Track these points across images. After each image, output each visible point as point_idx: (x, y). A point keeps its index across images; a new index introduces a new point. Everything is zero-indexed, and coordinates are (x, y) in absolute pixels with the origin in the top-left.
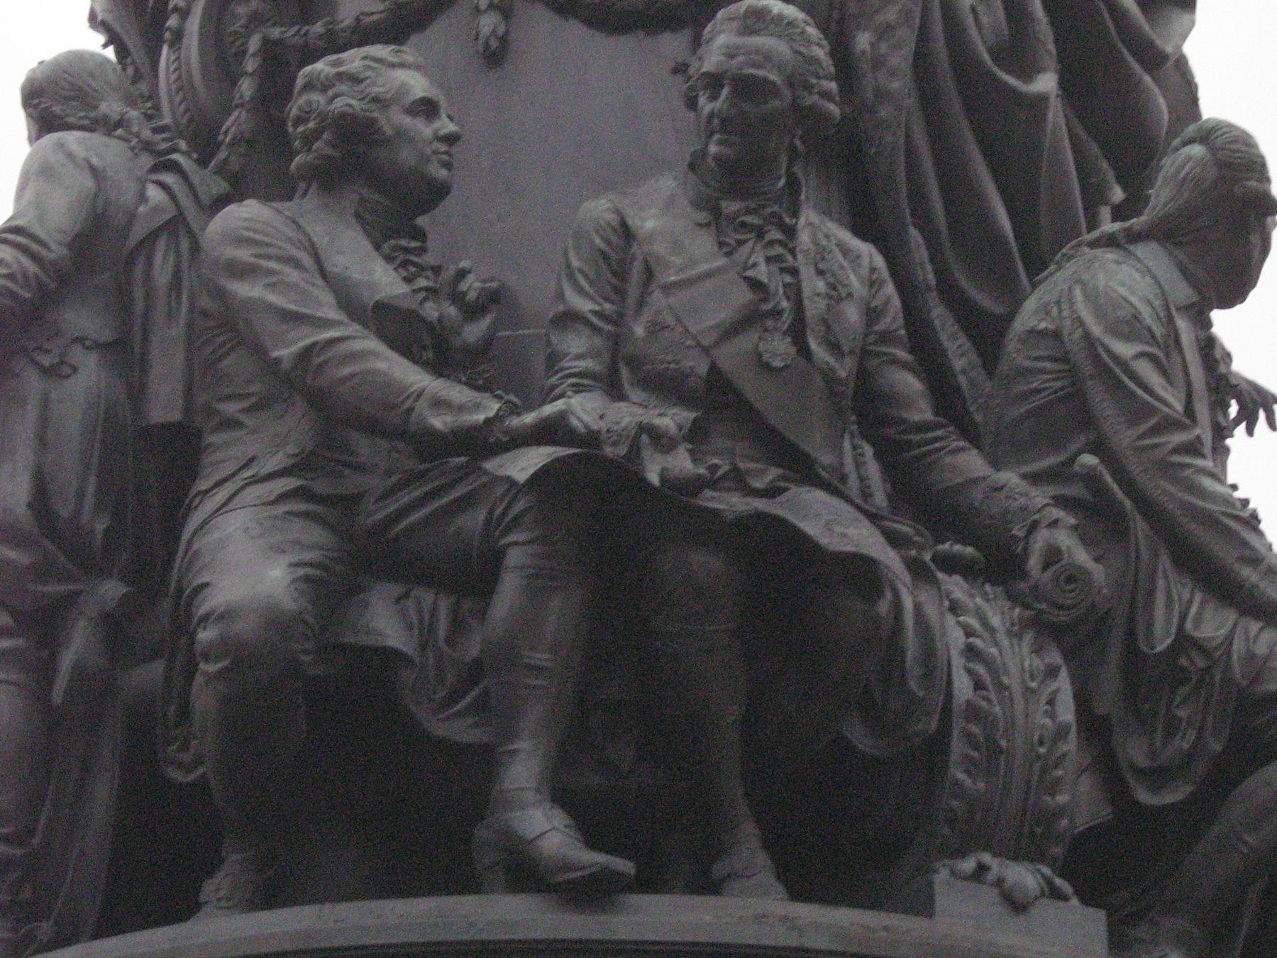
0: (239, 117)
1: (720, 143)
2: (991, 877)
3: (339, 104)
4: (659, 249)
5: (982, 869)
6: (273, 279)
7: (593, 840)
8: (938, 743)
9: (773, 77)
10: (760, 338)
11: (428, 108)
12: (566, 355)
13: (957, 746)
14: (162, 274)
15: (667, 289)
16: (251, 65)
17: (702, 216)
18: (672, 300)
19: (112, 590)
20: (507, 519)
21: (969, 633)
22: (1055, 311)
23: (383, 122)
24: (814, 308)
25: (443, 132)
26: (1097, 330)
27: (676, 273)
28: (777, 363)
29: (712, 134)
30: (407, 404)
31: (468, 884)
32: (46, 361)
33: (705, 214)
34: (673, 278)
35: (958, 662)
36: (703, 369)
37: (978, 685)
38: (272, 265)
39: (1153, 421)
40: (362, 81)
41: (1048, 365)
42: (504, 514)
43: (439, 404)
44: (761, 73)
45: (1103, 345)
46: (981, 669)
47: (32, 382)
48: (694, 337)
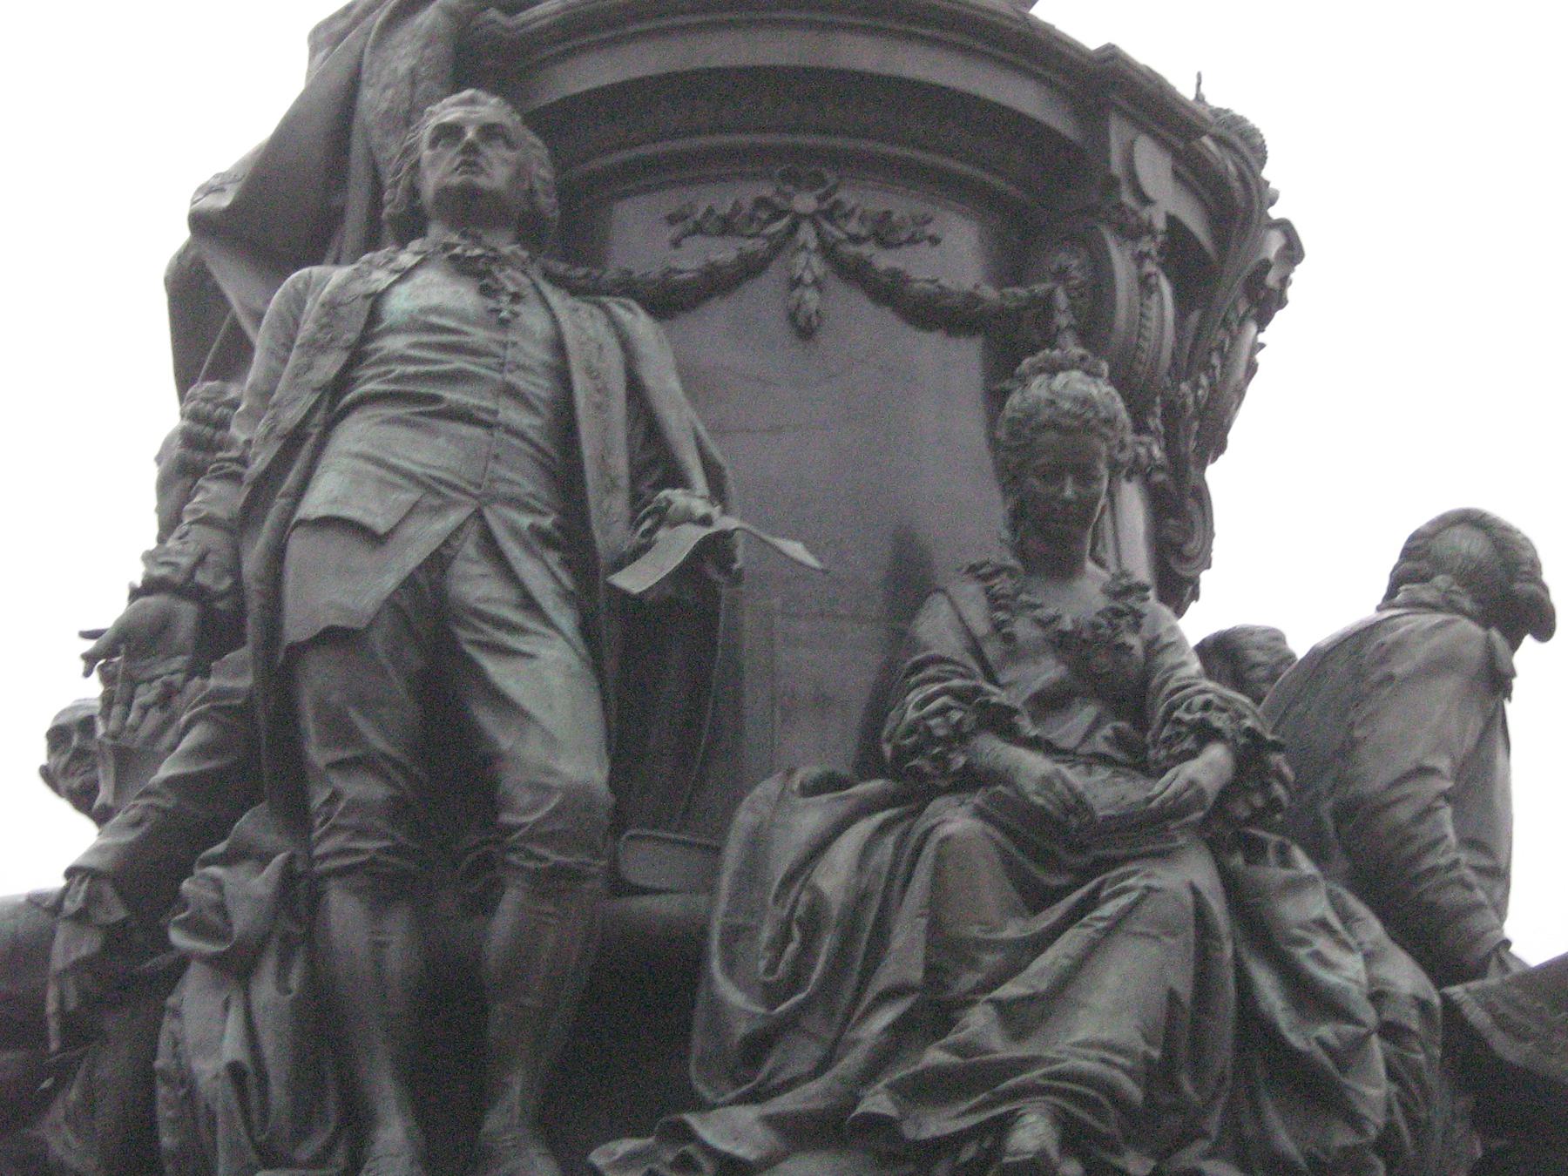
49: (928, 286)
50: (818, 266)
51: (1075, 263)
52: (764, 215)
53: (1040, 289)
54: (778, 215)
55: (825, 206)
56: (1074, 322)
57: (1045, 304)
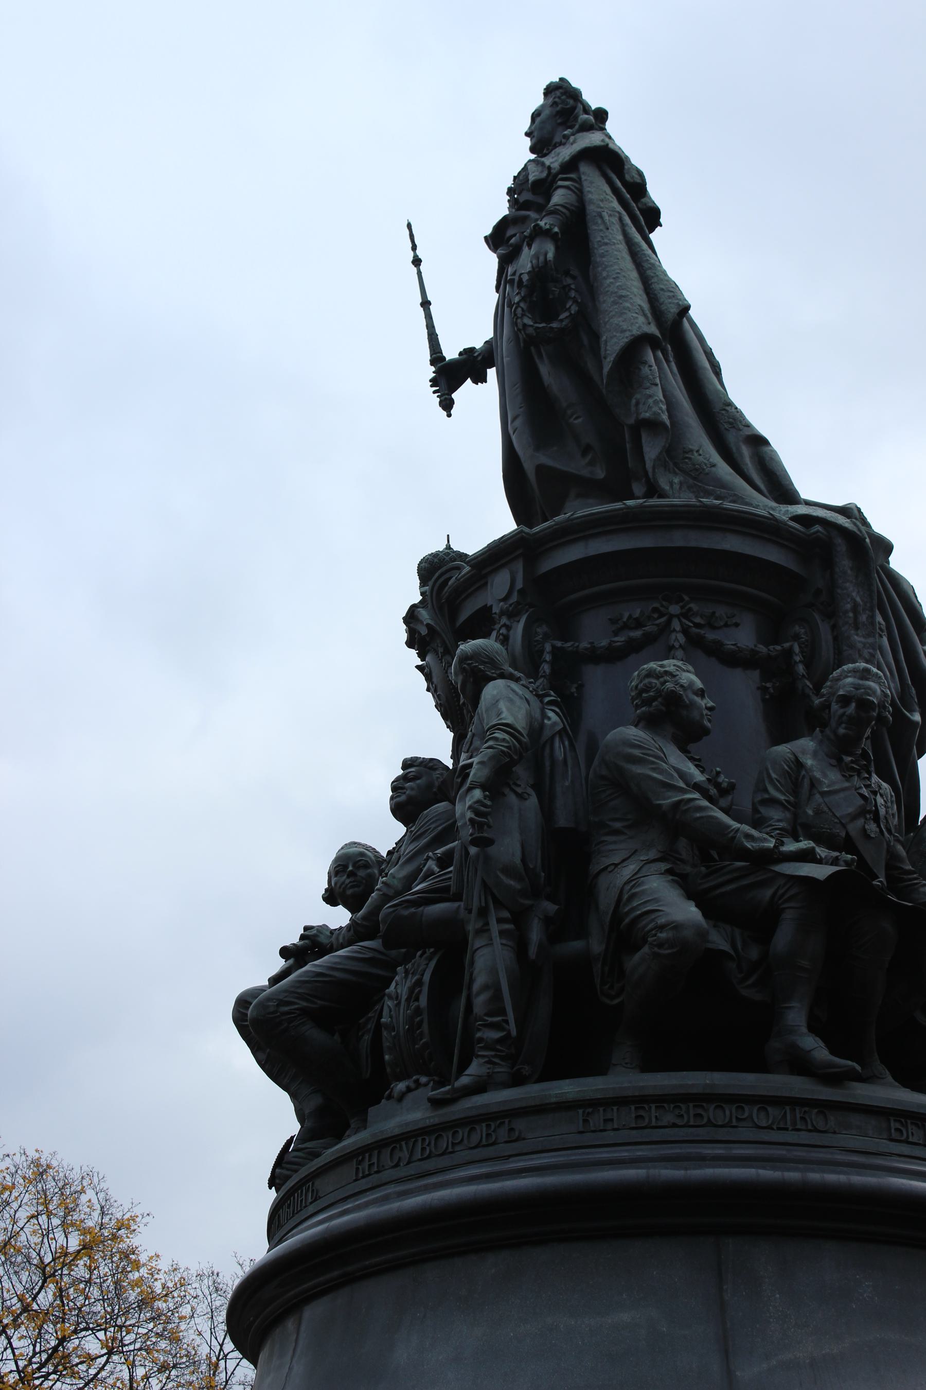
0: (543, 681)
1: (846, 728)
3: (669, 685)
4: (818, 775)
7: (832, 1052)
10: (865, 823)
11: (701, 693)
12: (773, 819)
14: (559, 753)
15: (823, 794)
16: (548, 657)
17: (834, 762)
18: (826, 799)
19: (550, 907)
20: (786, 897)
24: (882, 811)
25: (709, 705)
27: (827, 787)
28: (873, 835)
29: (842, 723)
30: (731, 835)
31: (761, 1066)
32: (519, 790)
33: (834, 761)
34: (826, 789)
36: (843, 834)
42: (783, 894)
43: (748, 837)
44: (871, 698)
47: (512, 798)
48: (838, 818)
49: (732, 647)
50: (682, 639)
51: (803, 631)
52: (656, 616)
53: (786, 645)
54: (662, 615)
55: (684, 611)
56: (803, 659)
57: (789, 653)
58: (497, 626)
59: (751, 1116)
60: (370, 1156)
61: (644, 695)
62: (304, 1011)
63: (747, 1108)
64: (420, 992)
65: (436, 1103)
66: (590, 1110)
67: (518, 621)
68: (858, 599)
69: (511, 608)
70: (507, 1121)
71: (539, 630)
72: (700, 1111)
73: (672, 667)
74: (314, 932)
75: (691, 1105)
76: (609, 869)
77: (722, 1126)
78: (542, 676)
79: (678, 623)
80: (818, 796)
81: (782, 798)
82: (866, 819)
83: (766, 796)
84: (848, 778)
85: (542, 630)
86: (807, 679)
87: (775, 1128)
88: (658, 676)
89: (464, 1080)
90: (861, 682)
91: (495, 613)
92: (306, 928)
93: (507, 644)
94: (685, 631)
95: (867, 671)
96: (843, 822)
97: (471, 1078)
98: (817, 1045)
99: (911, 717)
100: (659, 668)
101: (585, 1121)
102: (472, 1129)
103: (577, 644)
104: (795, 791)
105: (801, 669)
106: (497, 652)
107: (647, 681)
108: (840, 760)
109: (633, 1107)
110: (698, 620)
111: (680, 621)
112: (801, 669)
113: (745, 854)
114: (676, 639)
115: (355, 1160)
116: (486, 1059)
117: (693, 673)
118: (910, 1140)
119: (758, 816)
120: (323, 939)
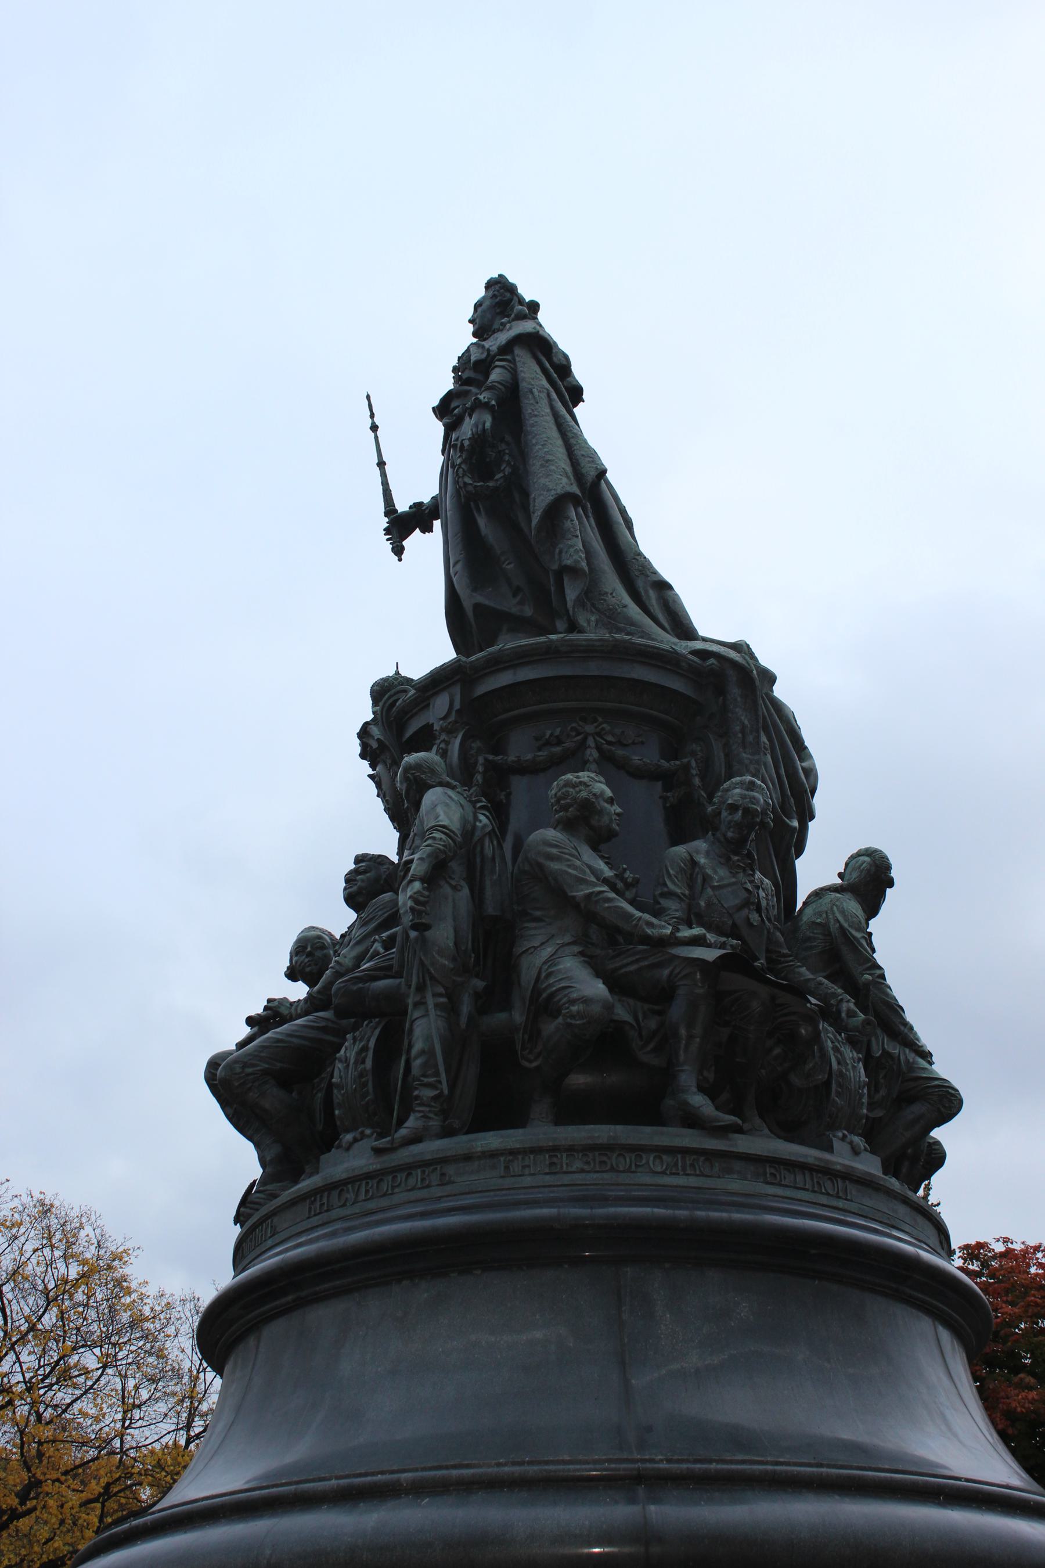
1: (733, 832)
2: (848, 1140)
3: (583, 794)
4: (709, 871)
5: (845, 1136)
6: (569, 863)
8: (828, 1083)
9: (759, 809)
10: (749, 913)
11: (611, 801)
13: (834, 1086)
14: (488, 851)
15: (713, 888)
16: (481, 769)
17: (722, 860)
18: (717, 893)
21: (832, 1042)
22: (824, 915)
23: (597, 804)
24: (764, 903)
25: (617, 811)
26: (846, 925)
27: (717, 882)
28: (755, 924)
32: (453, 883)
34: (716, 884)
35: (831, 1052)
36: (730, 922)
37: (839, 1063)
38: (567, 856)
39: (870, 964)
40: (589, 786)
41: (820, 936)
43: (650, 925)
44: (755, 807)
45: (849, 931)
46: (839, 1056)
47: (447, 890)
48: (726, 909)
49: (639, 762)
50: (596, 754)
51: (699, 748)
52: (574, 734)
53: (685, 760)
54: (578, 734)
55: (598, 730)
56: (698, 773)
57: (687, 767)
58: (438, 741)
59: (648, 1163)
60: (321, 1197)
61: (562, 802)
62: (266, 1072)
63: (644, 1156)
64: (366, 1056)
65: (378, 1151)
66: (511, 1158)
67: (456, 737)
68: (746, 722)
69: (449, 727)
70: (439, 1167)
71: (474, 745)
72: (605, 1158)
73: (586, 778)
74: (276, 1003)
75: (597, 1153)
76: (530, 952)
77: (623, 1172)
78: (476, 785)
79: (593, 740)
80: (709, 890)
81: (679, 891)
82: (750, 909)
83: (666, 889)
84: (734, 875)
85: (476, 744)
86: (702, 790)
87: (668, 1172)
88: (574, 786)
89: (403, 1132)
90: (747, 793)
91: (436, 730)
92: (269, 1001)
93: (446, 757)
94: (598, 748)
95: (752, 783)
96: (730, 912)
97: (408, 1130)
98: (704, 1102)
99: (790, 823)
100: (575, 779)
101: (507, 1168)
102: (409, 1174)
103: (506, 758)
104: (691, 887)
105: (697, 781)
106: (436, 764)
107: (564, 790)
108: (729, 859)
109: (547, 1156)
110: (610, 738)
111: (594, 738)
112: (697, 781)
113: (646, 939)
114: (591, 755)
115: (308, 1201)
116: (422, 1114)
117: (604, 783)
118: (783, 1183)
119: (658, 906)
120: (284, 1011)
